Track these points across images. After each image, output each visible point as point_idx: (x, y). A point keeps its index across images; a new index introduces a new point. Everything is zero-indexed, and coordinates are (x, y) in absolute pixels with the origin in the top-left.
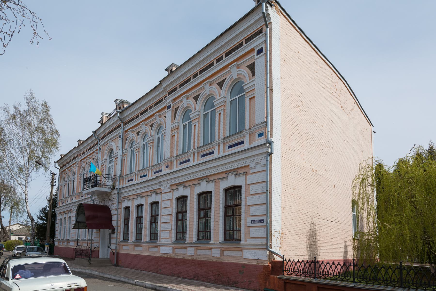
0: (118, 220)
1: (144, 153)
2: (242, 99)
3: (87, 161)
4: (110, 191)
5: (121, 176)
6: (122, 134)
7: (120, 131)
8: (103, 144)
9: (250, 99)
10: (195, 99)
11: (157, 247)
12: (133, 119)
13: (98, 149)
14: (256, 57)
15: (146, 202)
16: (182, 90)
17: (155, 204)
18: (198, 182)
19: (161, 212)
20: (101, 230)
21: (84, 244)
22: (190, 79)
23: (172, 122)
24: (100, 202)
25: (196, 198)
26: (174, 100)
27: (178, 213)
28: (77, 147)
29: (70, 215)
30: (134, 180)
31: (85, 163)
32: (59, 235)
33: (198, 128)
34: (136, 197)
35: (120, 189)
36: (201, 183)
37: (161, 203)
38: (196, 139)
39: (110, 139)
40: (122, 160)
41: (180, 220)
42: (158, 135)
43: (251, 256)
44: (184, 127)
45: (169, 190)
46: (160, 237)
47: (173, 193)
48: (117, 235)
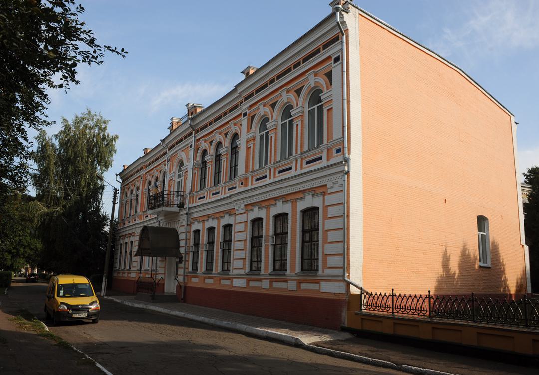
2: (320, 109)
4: (178, 211)
7: (192, 140)
8: (172, 154)
9: (328, 110)
10: (272, 107)
11: (229, 279)
13: (166, 160)
14: (333, 65)
16: (258, 96)
17: (228, 228)
19: (235, 237)
20: (167, 258)
21: (147, 276)
23: (248, 131)
24: (166, 224)
25: (272, 220)
27: (253, 238)
29: (132, 239)
30: (205, 197)
31: (151, 176)
34: (207, 219)
35: (189, 208)
36: (277, 204)
39: (180, 149)
43: (328, 288)
44: (261, 137)
45: (243, 211)
48: (185, 264)
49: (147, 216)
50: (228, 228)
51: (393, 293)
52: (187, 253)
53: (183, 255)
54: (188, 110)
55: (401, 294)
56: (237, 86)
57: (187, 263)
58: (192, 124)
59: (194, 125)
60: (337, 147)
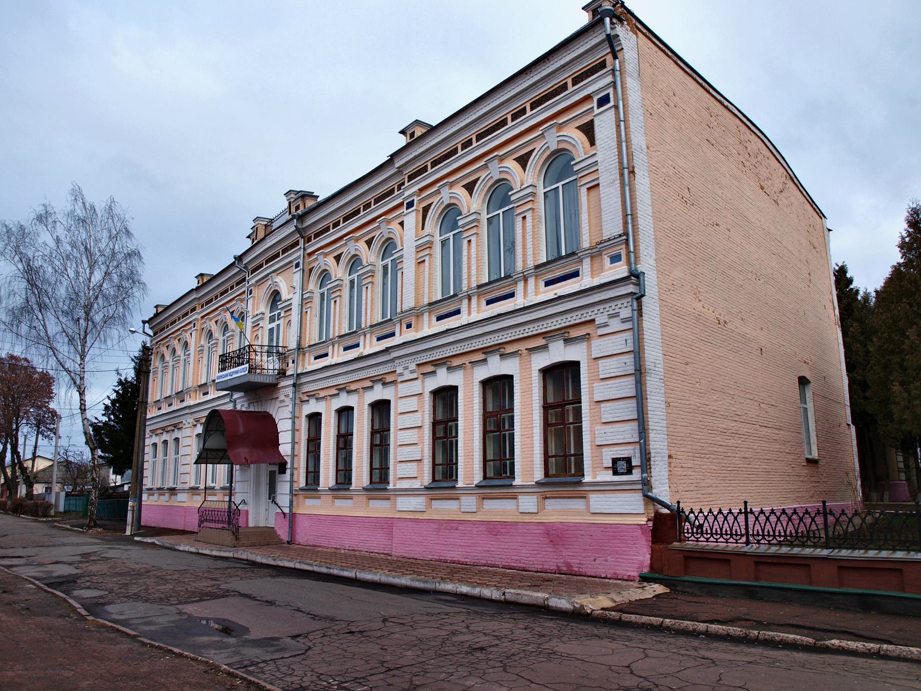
0: (294, 443)
1: (351, 297)
3: (219, 318)
5: (299, 348)
6: (301, 261)
7: (297, 254)
8: (257, 282)
9: (589, 189)
10: (467, 189)
12: (327, 229)
15: (361, 405)
18: (482, 357)
22: (456, 149)
25: (477, 390)
26: (421, 190)
27: (435, 424)
28: (197, 289)
29: (177, 434)
30: (330, 354)
31: (213, 322)
32: (150, 479)
33: (477, 246)
35: (298, 375)
37: (396, 403)
38: (474, 267)
40: (302, 314)
41: (441, 438)
42: (382, 260)
44: (444, 243)
45: (414, 376)
46: (395, 474)
47: (423, 381)
49: (207, 393)
50: (381, 408)
51: (746, 508)
52: (293, 456)
53: (288, 460)
54: (290, 203)
55: (754, 510)
56: (393, 156)
57: (295, 472)
58: (300, 227)
59: (303, 229)
60: (613, 251)
